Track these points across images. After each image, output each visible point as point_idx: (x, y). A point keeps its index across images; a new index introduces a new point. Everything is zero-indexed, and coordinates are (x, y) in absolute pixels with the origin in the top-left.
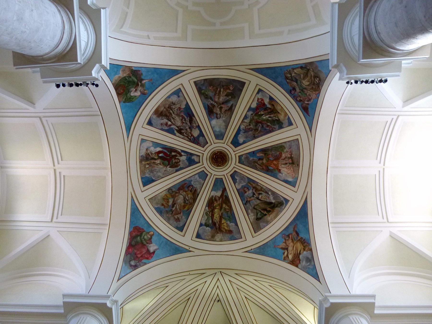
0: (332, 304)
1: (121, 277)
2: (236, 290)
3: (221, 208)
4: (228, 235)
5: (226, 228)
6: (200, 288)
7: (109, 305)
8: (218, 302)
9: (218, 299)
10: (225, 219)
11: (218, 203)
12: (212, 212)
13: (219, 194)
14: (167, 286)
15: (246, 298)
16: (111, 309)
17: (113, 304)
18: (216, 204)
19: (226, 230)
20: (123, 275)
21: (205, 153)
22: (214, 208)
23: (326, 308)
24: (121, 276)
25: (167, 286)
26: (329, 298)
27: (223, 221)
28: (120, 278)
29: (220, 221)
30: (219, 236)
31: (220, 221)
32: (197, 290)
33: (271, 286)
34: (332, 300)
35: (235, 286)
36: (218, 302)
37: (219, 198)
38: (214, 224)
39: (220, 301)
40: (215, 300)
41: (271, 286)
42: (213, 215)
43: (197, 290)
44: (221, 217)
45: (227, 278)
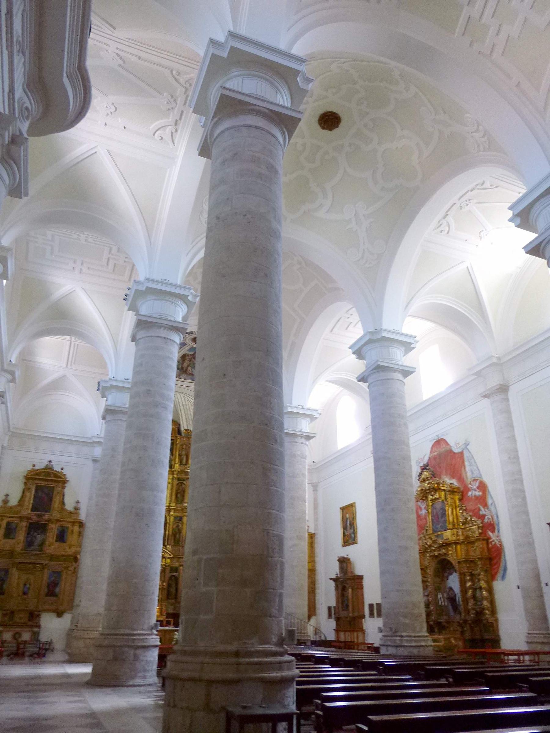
2: (186, 401)
3: (190, 361)
4: (191, 377)
5: (190, 372)
10: (191, 367)
11: (190, 357)
12: (183, 362)
13: (192, 353)
18: (187, 358)
19: (190, 373)
21: (189, 337)
22: (186, 360)
27: (189, 368)
29: (187, 368)
30: (184, 376)
31: (187, 368)
35: (186, 399)
37: (191, 355)
38: (182, 368)
42: (182, 364)
44: (188, 366)
45: (182, 395)
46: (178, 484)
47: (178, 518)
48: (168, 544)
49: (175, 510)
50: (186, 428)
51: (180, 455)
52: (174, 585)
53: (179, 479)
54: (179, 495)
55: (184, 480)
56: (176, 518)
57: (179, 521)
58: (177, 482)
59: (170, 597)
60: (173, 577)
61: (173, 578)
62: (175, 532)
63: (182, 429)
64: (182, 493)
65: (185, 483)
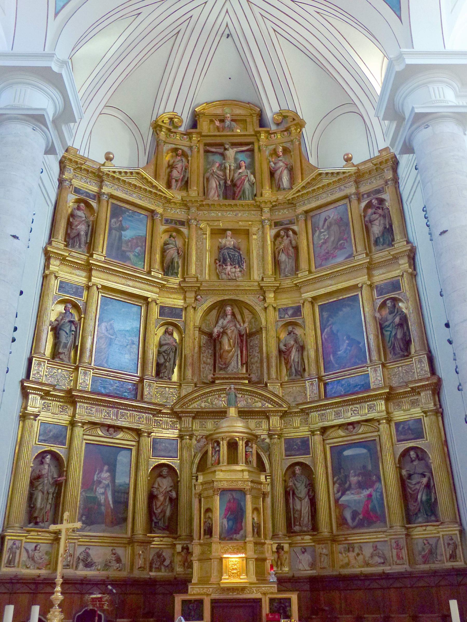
0: (408, 66)
1: (60, 8)
6: (195, 13)
7: (55, 69)
8: (227, 37)
9: (227, 32)
14: (140, 14)
15: (274, 30)
16: (61, 75)
17: (61, 67)
20: (62, 4)
23: (397, 72)
24: (58, 8)
25: (140, 14)
26: (405, 56)
28: (57, 10)
32: (191, 17)
33: (318, 13)
34: (409, 61)
36: (227, 37)
39: (230, 37)
40: (223, 34)
41: (318, 13)
43: (191, 17)
46: (277, 236)
47: (290, 312)
48: (269, 378)
49: (277, 290)
50: (276, 109)
51: (272, 174)
52: (302, 491)
53: (276, 224)
54: (283, 257)
55: (291, 223)
56: (282, 311)
57: (293, 319)
58: (274, 232)
59: (297, 528)
60: (297, 467)
61: (298, 469)
62: (285, 345)
63: (269, 115)
64: (291, 251)
65: (295, 228)
